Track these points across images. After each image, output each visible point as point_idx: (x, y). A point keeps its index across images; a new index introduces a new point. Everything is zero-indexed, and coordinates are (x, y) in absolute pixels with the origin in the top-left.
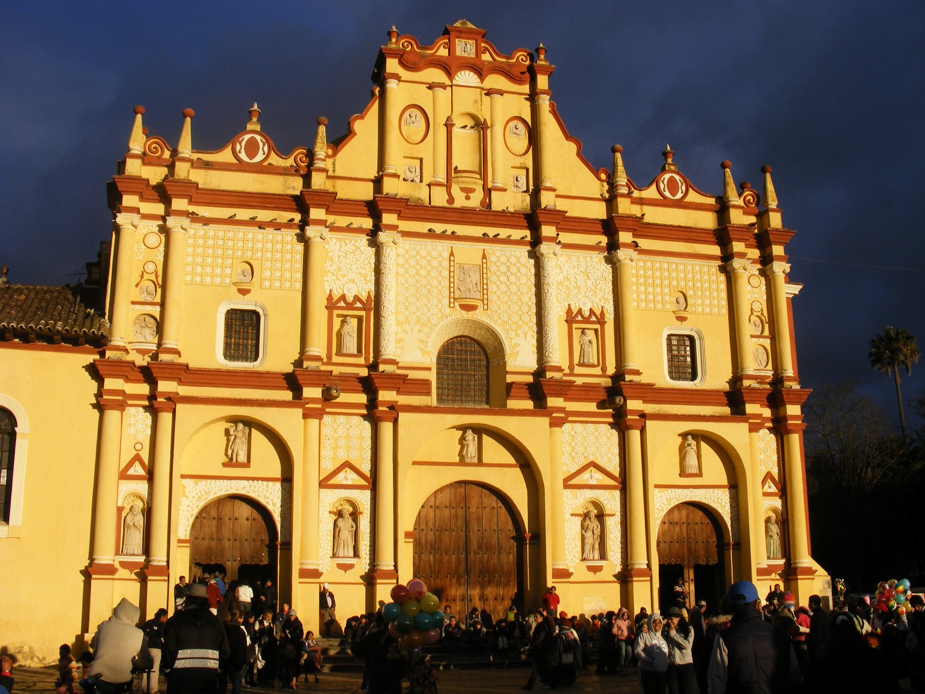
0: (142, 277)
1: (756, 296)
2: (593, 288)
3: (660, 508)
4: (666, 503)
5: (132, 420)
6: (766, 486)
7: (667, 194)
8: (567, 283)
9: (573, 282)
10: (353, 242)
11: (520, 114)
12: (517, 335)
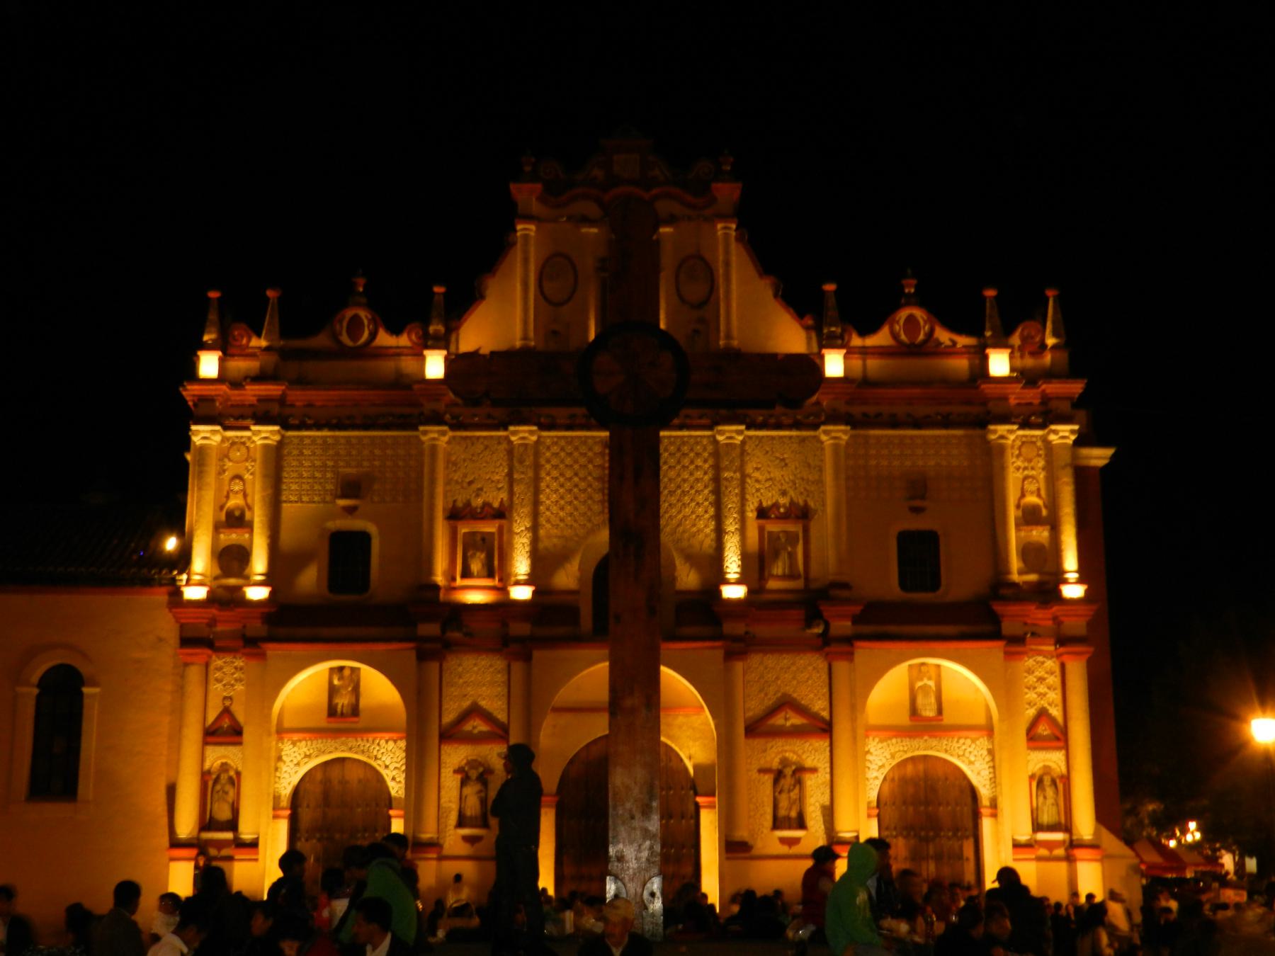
0: (228, 497)
7: (903, 337)
8: (756, 475)
10: (481, 440)
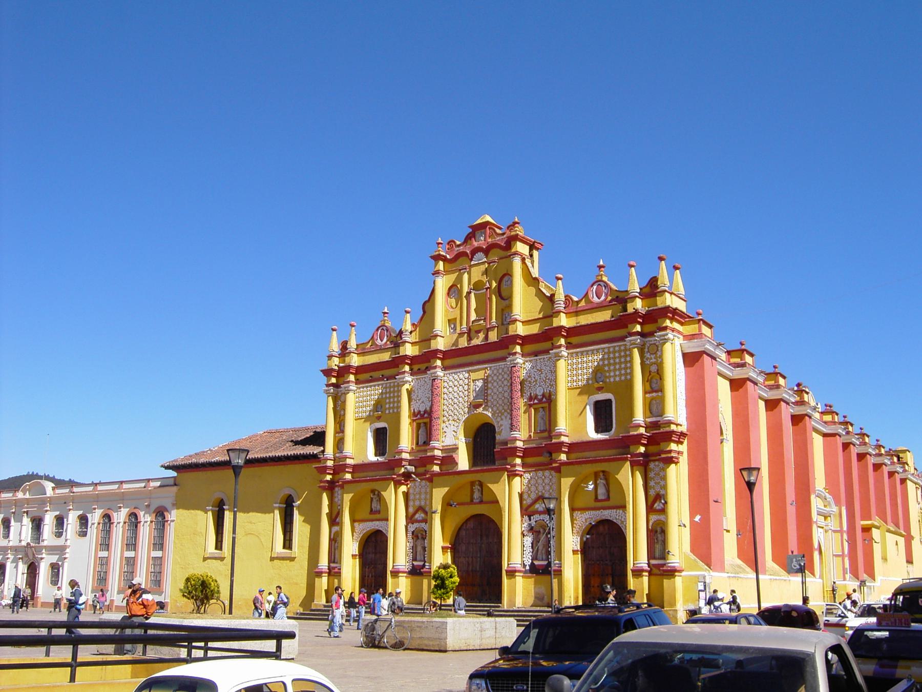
1: (653, 360)
2: (544, 379)
3: (580, 525)
4: (584, 521)
5: (336, 495)
6: (656, 505)
7: (596, 299)
8: (529, 379)
9: (533, 378)
11: (507, 271)
12: (502, 419)
